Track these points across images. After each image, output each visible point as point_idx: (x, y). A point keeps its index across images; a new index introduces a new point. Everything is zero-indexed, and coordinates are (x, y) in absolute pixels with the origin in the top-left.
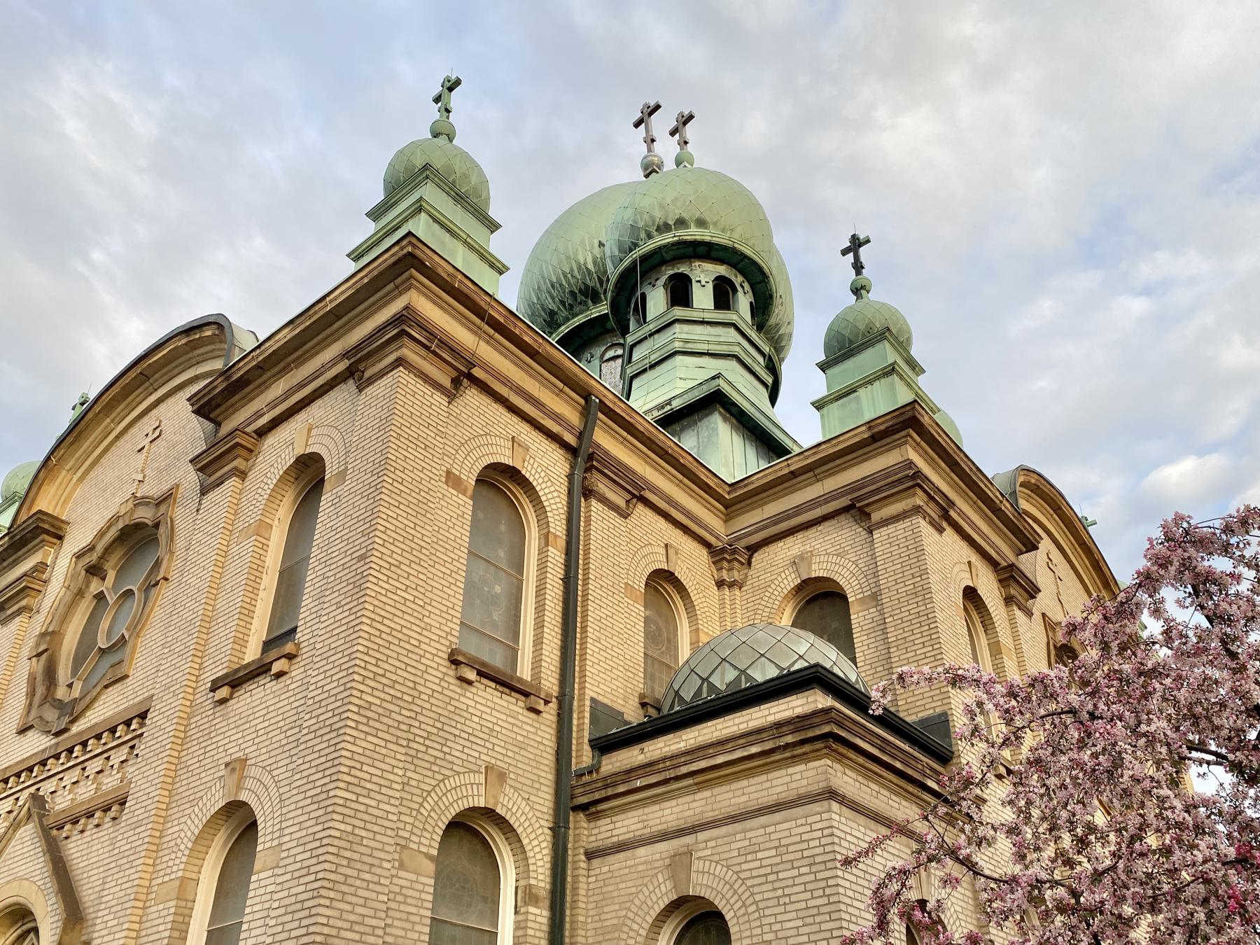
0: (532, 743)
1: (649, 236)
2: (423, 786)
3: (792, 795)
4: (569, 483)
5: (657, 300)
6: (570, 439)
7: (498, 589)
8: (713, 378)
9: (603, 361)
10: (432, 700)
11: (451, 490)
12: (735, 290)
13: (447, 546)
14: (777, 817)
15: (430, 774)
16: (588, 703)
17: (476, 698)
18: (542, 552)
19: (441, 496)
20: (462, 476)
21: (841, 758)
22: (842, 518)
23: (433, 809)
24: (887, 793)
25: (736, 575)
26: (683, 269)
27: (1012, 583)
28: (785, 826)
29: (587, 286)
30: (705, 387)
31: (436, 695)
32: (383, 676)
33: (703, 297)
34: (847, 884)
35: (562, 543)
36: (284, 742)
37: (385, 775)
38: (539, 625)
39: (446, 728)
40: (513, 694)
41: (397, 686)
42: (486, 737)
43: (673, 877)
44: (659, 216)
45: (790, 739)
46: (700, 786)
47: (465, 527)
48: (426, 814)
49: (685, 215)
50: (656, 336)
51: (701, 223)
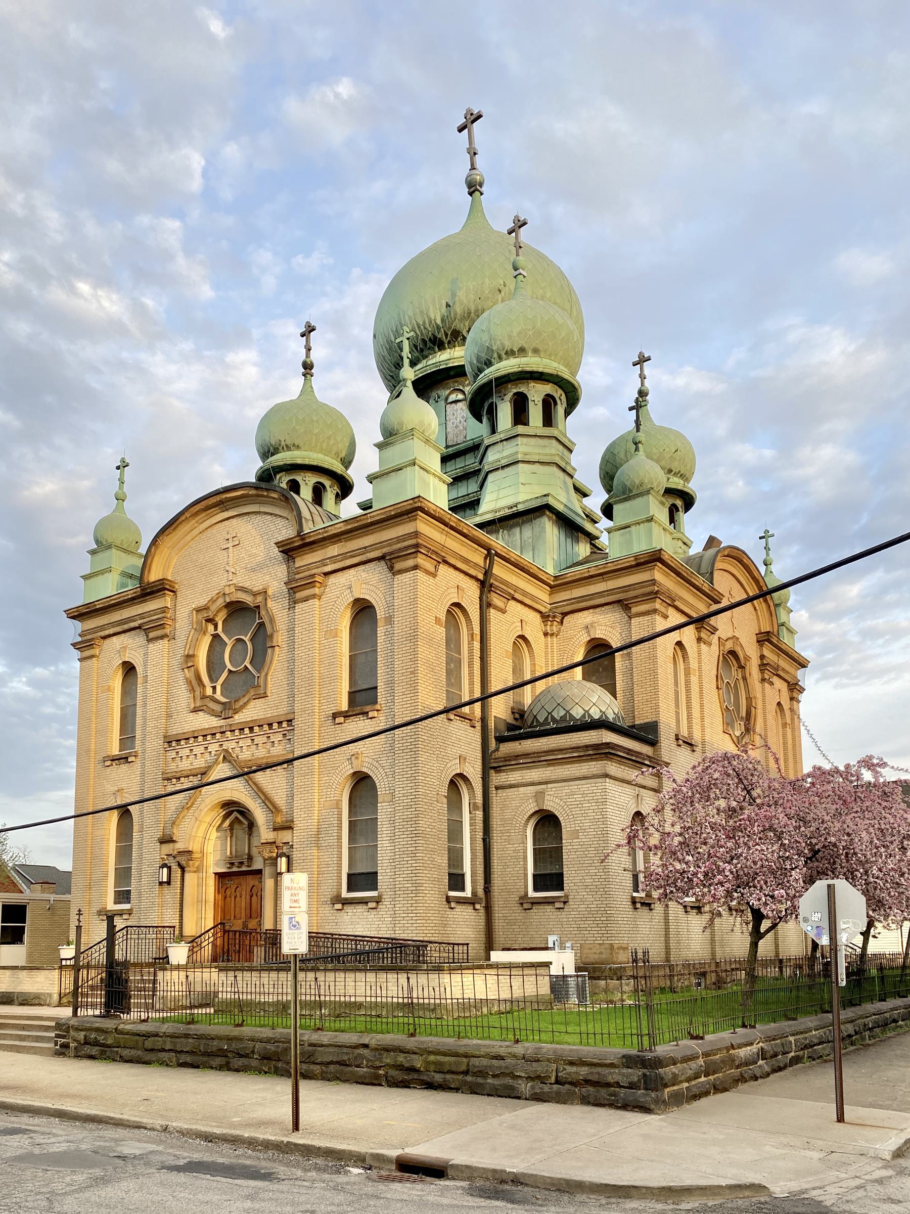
1: (500, 358)
3: (589, 774)
4: (480, 601)
5: (505, 413)
6: (481, 577)
8: (545, 496)
9: (447, 403)
12: (556, 403)
14: (584, 782)
16: (493, 719)
18: (470, 643)
21: (611, 760)
22: (615, 605)
24: (627, 768)
25: (555, 629)
26: (522, 389)
27: (703, 630)
28: (585, 786)
29: (435, 337)
30: (539, 500)
33: (535, 413)
34: (610, 810)
35: (478, 637)
36: (383, 749)
38: (471, 683)
40: (466, 721)
43: (536, 801)
44: (508, 345)
45: (591, 752)
46: (549, 765)
49: (525, 345)
50: (504, 442)
51: (536, 351)
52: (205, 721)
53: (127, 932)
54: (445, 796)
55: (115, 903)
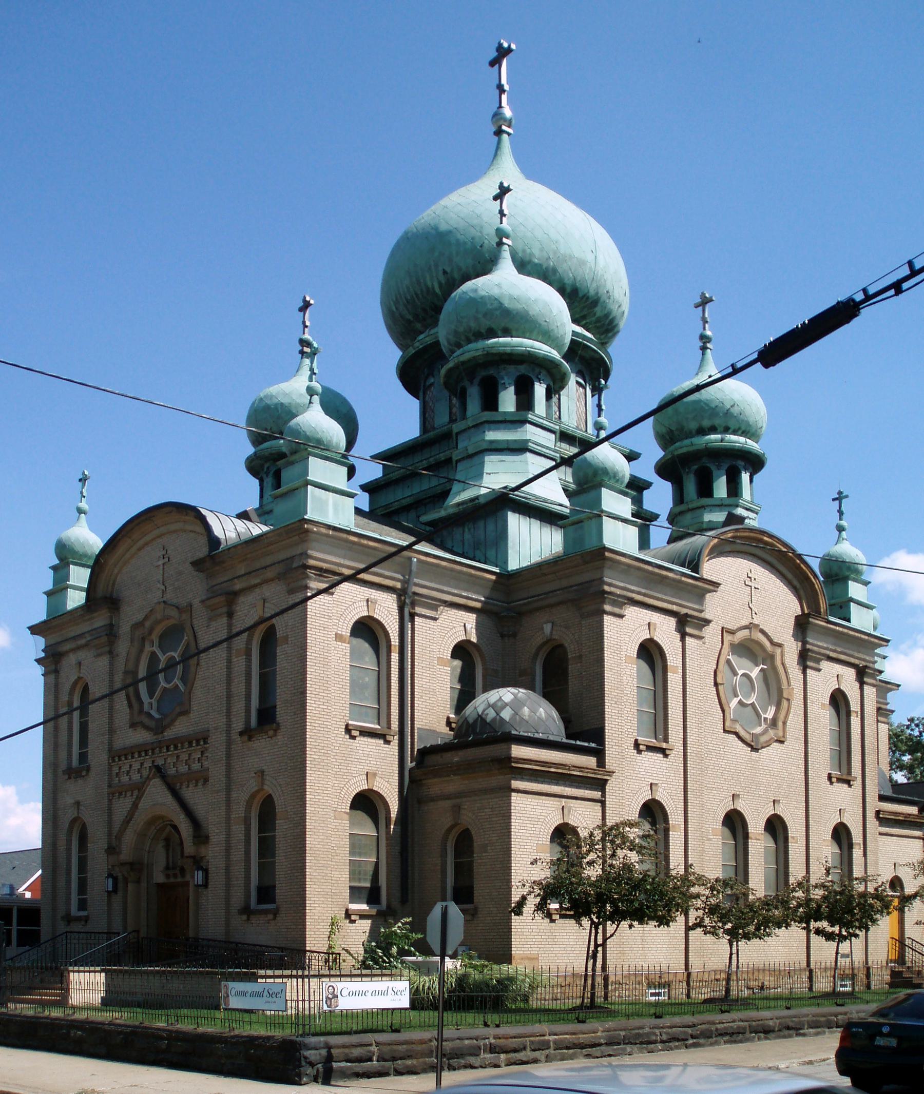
0: (388, 756)
2: (340, 785)
7: (367, 679)
10: (341, 749)
11: (338, 643)
13: (339, 673)
15: (343, 780)
17: (360, 742)
19: (333, 648)
20: (344, 633)
23: (345, 794)
31: (342, 746)
32: (319, 745)
37: (324, 786)
39: (347, 759)
41: (325, 748)
42: (366, 758)
47: (347, 660)
48: (342, 796)
52: (141, 736)
53: (67, 937)
54: (345, 813)
55: (79, 910)
